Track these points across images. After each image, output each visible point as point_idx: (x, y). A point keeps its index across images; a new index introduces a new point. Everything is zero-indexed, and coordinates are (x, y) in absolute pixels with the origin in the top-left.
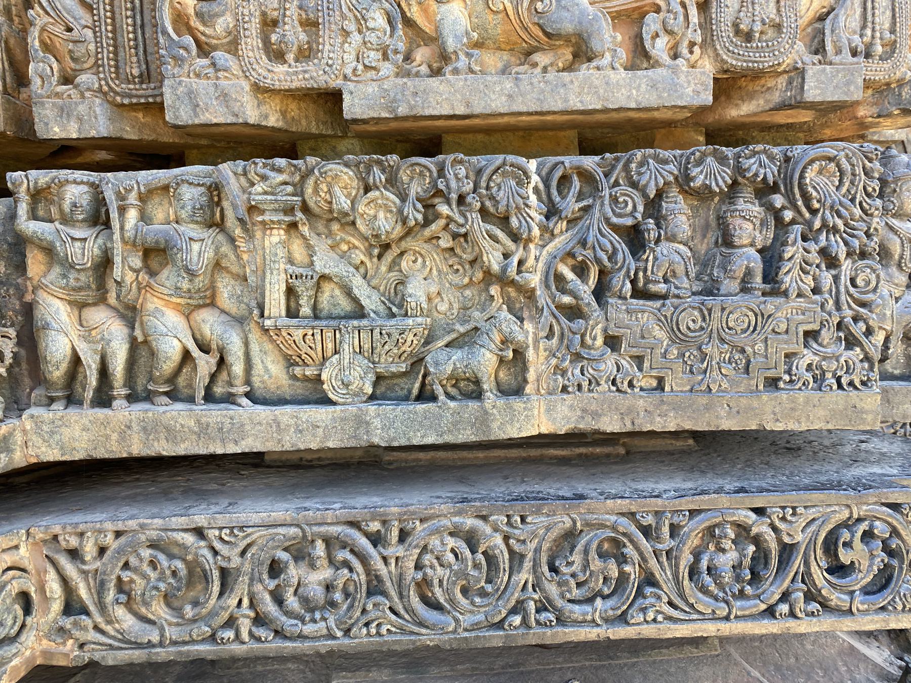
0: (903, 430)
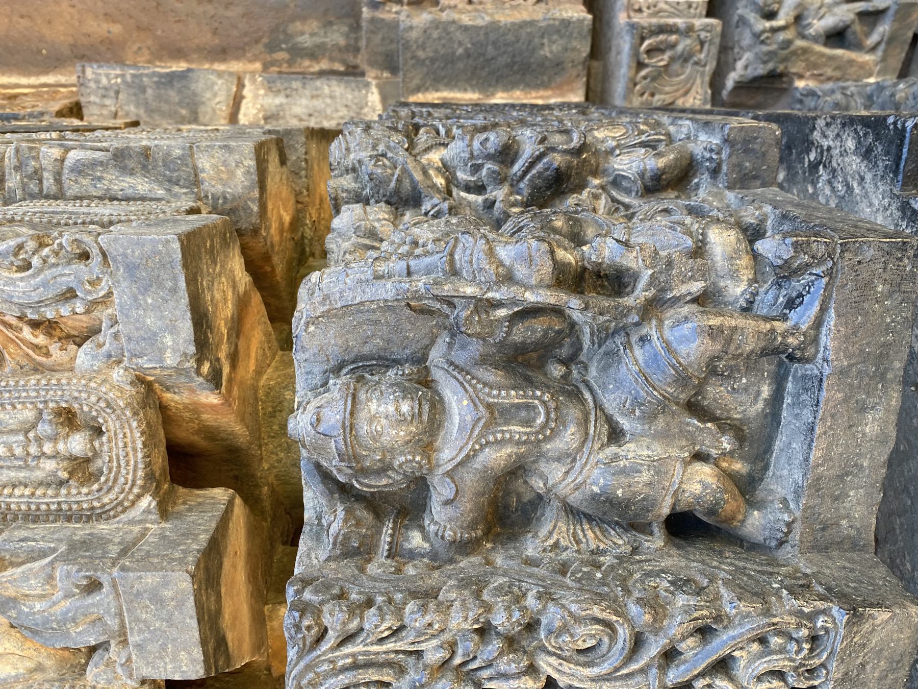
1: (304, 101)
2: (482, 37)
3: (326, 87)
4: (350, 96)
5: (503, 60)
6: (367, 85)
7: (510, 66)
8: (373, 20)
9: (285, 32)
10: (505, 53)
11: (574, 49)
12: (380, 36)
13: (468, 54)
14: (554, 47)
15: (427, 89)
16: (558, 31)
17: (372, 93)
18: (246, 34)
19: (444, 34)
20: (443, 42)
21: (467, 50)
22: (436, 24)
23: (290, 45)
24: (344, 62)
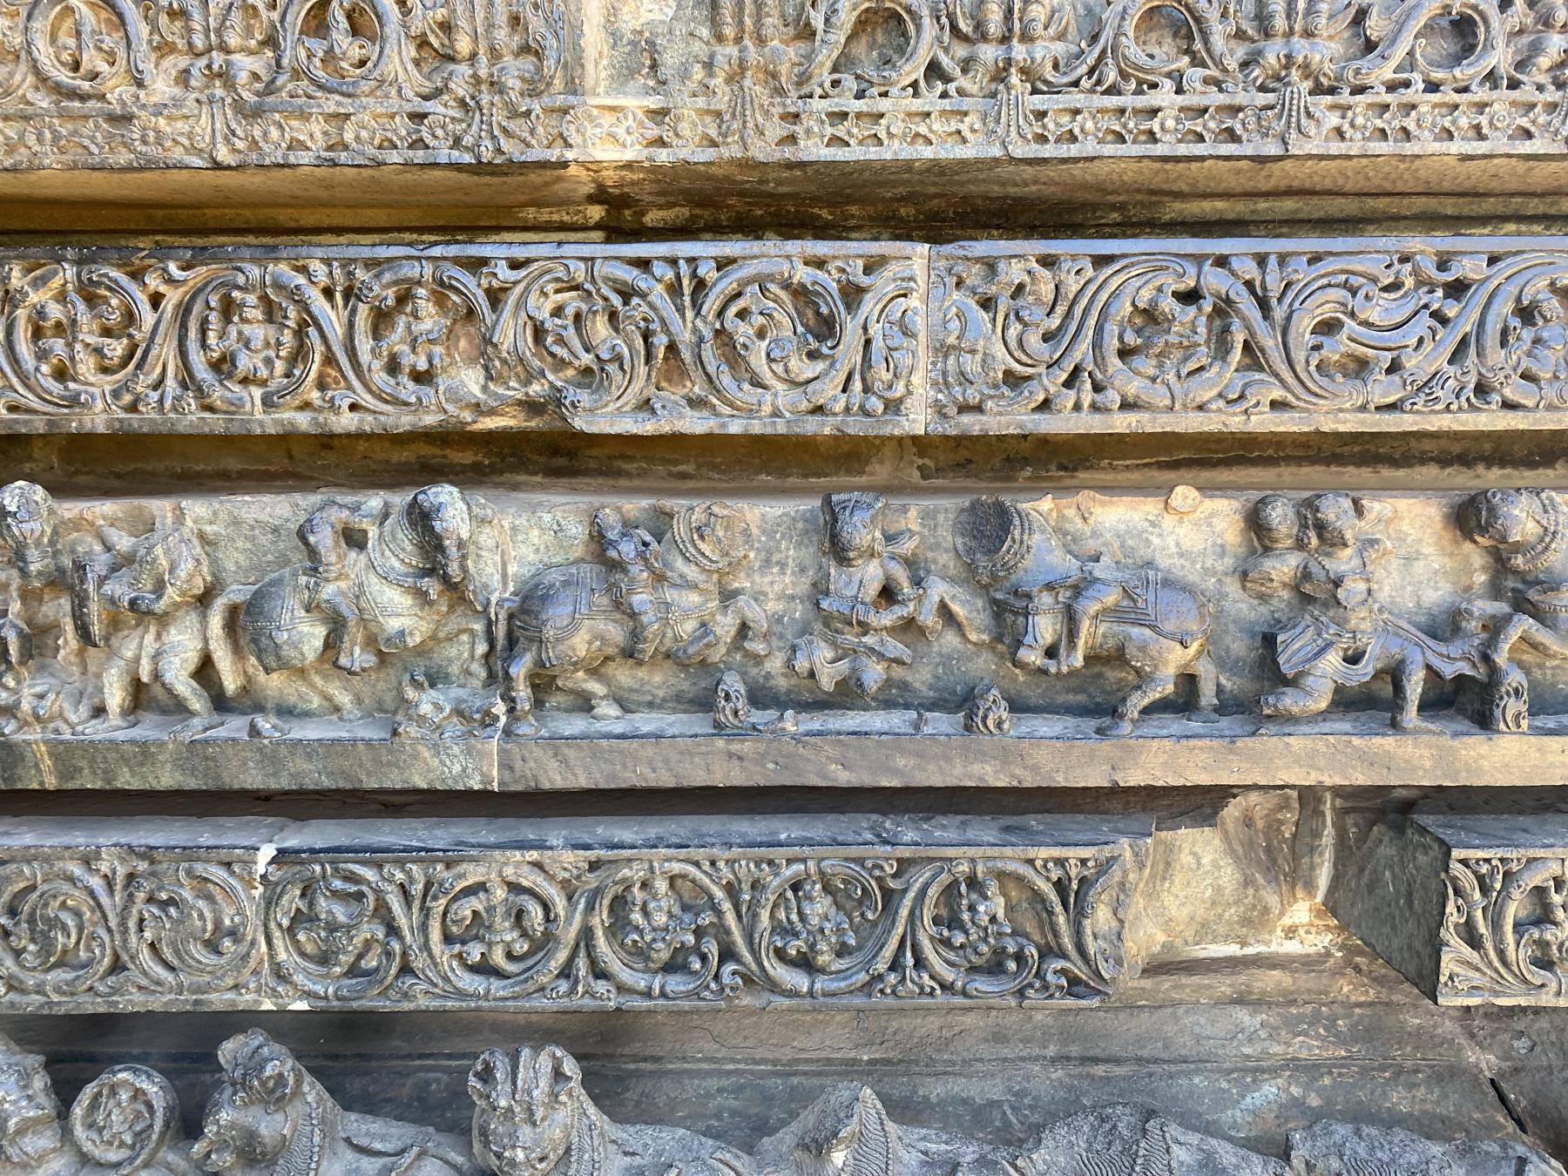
0: (155, 396)
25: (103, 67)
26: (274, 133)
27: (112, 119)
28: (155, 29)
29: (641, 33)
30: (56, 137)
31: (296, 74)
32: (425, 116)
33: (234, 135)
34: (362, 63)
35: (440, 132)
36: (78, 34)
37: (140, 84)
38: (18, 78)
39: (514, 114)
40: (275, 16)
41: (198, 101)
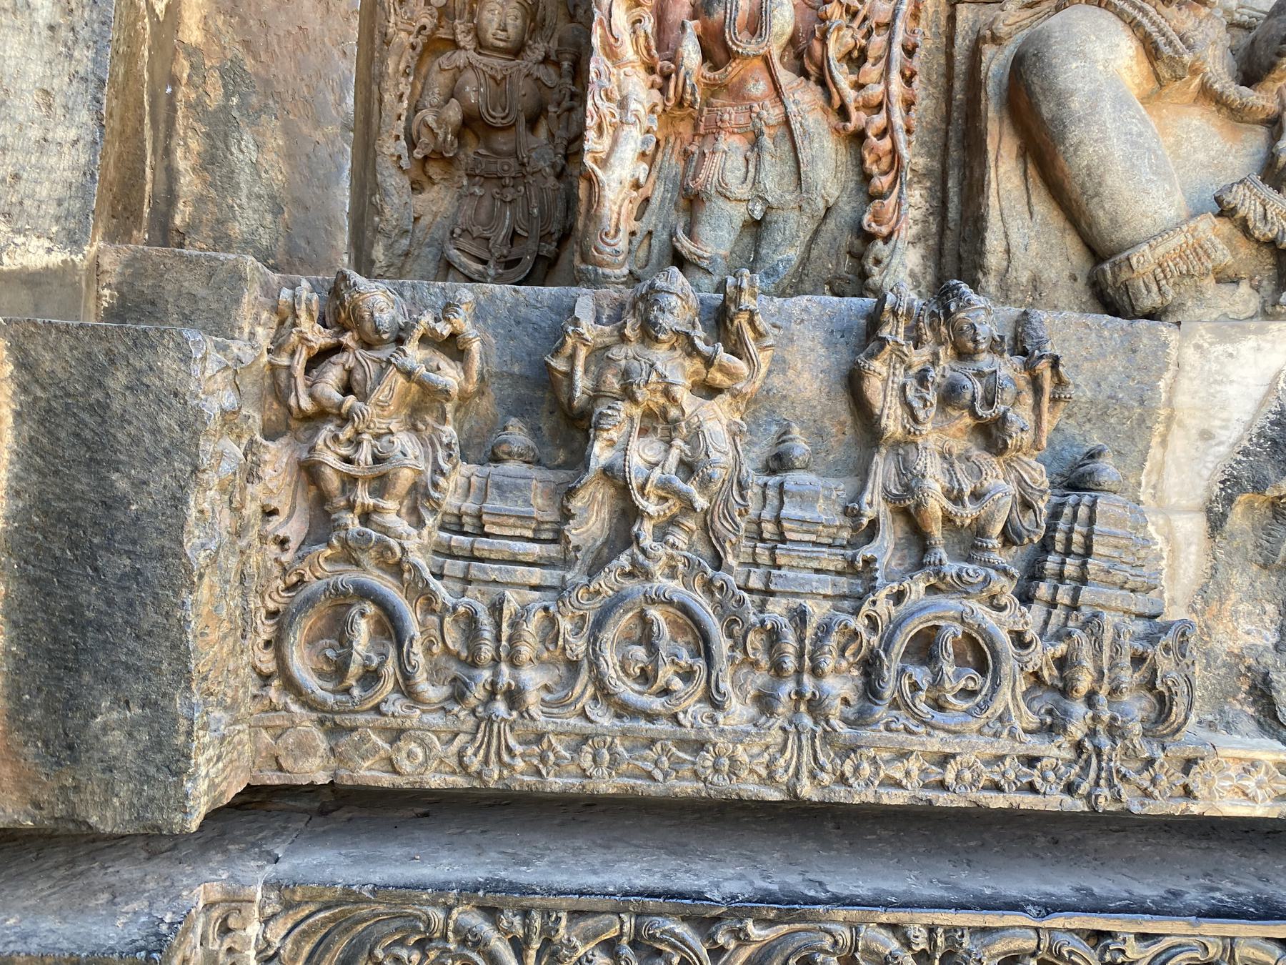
1: (36, 70)
2: (155, 542)
3: (73, 134)
4: (43, 191)
5: (90, 596)
6: (73, 240)
7: (75, 618)
8: (237, 278)
9: (264, 109)
10: (110, 602)
11: (109, 789)
12: (201, 291)
13: (112, 503)
14: (117, 735)
15: (24, 389)
16: (158, 744)
17: (49, 251)
18: (264, 24)
19: (166, 443)
20: (147, 438)
21: (124, 501)
22: (192, 424)
23: (235, 113)
24: (193, 227)
25: (677, 684)
26: (867, 769)
27: (682, 743)
28: (739, 643)
29: (1240, 657)
30: (614, 763)
31: (894, 705)
32: (1038, 759)
33: (822, 769)
34: (968, 694)
35: (1051, 776)
36: (653, 650)
37: (717, 706)
38: (578, 690)
39: (1130, 754)
40: (875, 640)
41: (783, 729)
